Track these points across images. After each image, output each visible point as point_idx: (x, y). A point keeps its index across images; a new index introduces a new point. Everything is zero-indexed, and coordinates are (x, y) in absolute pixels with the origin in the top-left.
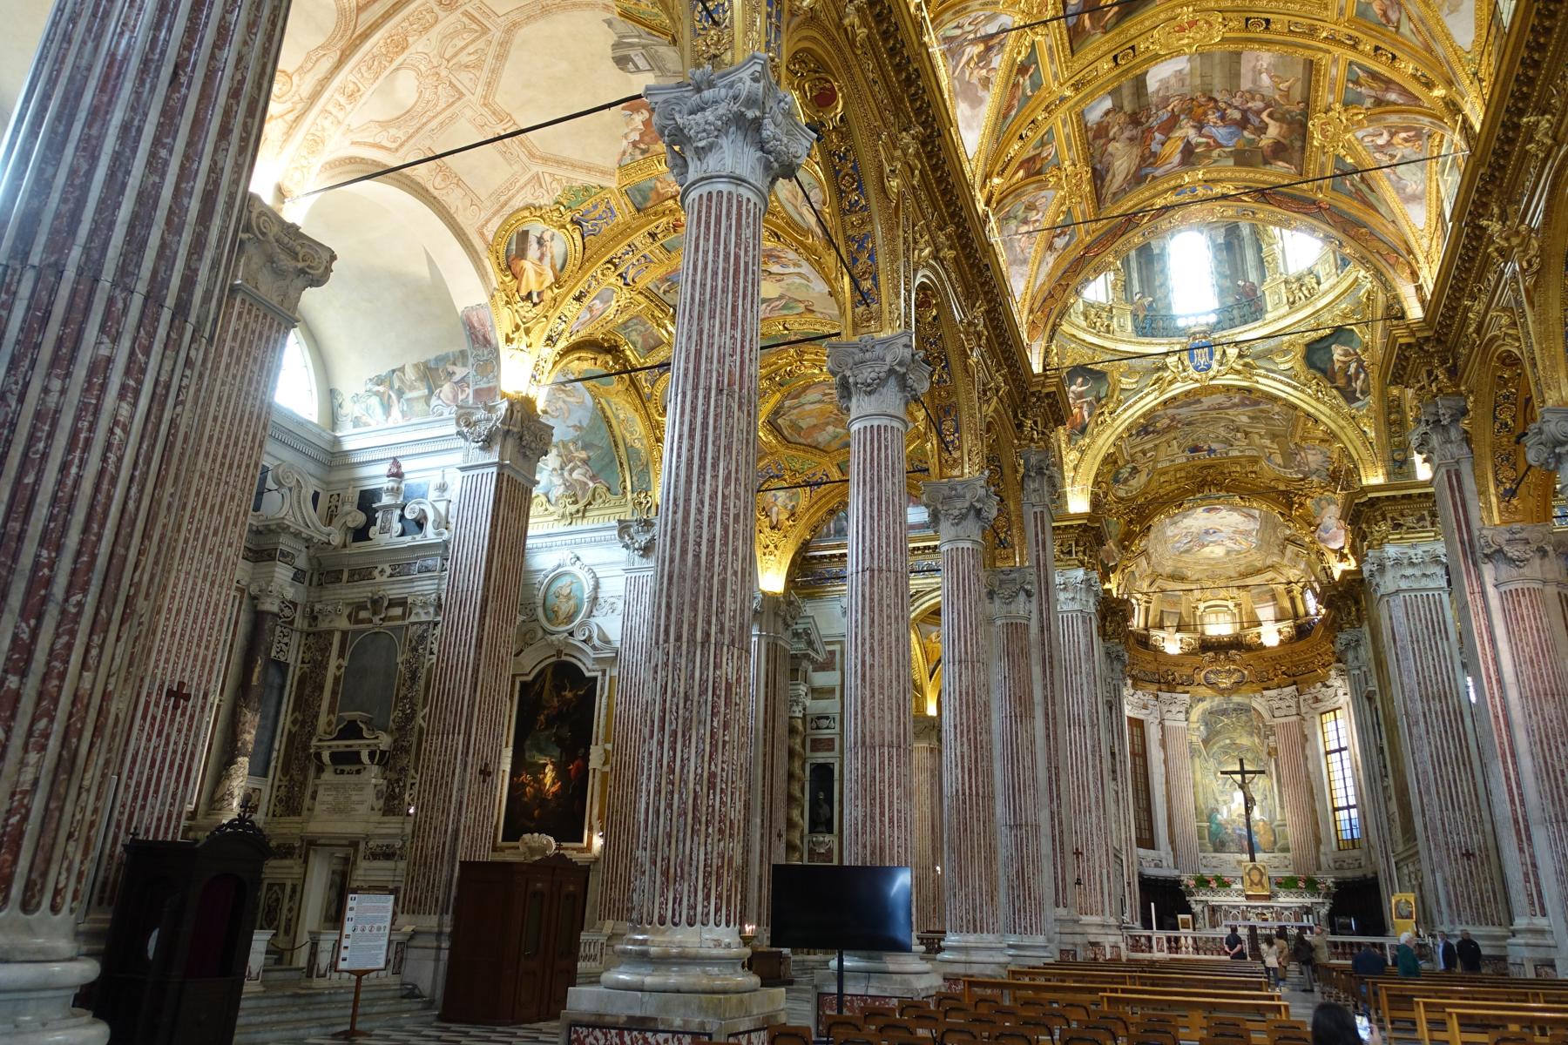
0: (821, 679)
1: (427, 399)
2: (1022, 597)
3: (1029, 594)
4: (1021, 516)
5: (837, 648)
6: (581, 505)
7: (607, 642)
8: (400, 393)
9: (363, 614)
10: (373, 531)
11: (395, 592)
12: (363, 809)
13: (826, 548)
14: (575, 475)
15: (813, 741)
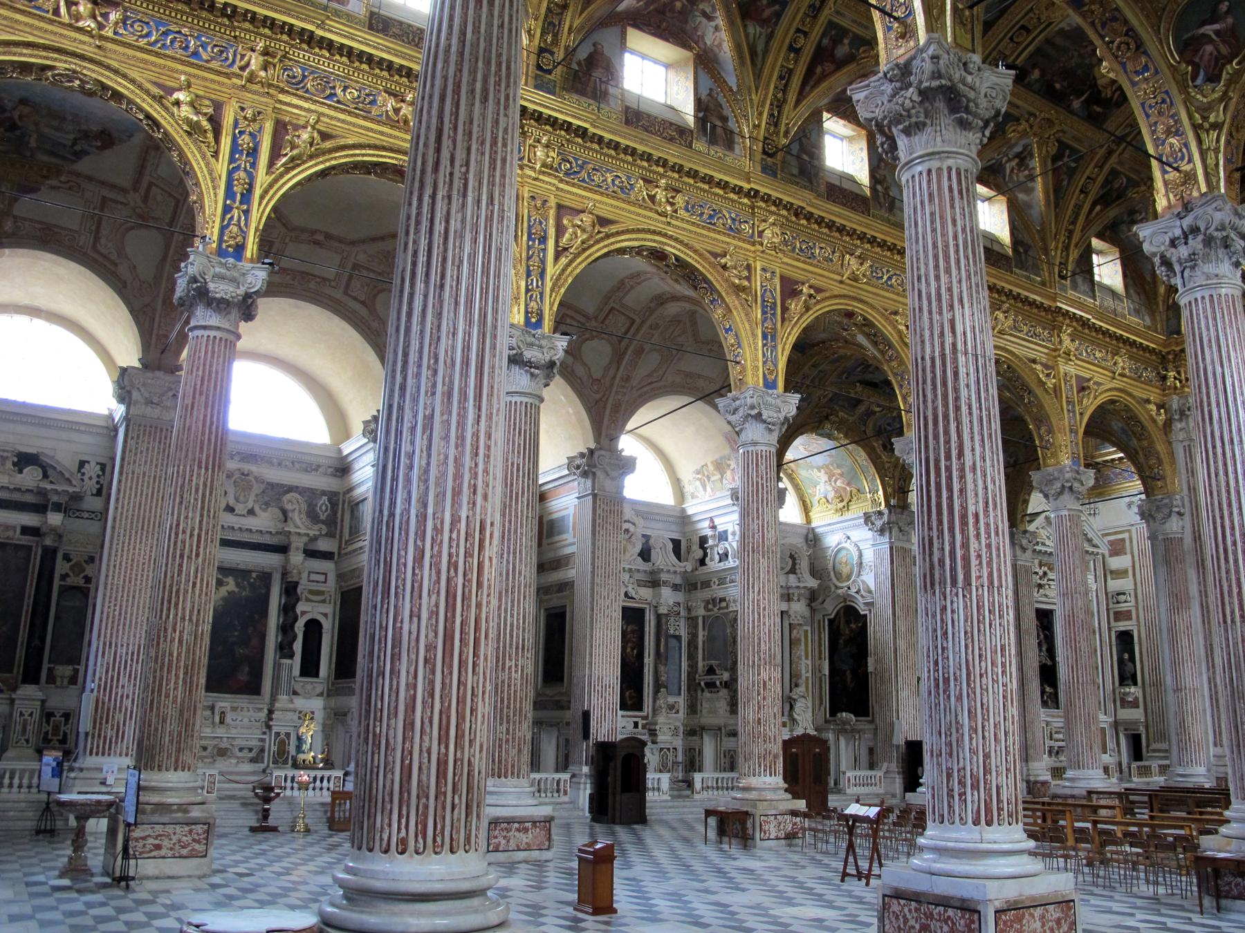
0: (1116, 563)
1: (721, 480)
2: (1174, 518)
3: (1180, 514)
4: (1172, 454)
5: (1126, 535)
6: (844, 503)
7: (870, 592)
8: (708, 478)
9: (710, 606)
10: (707, 560)
11: (721, 594)
12: (721, 711)
13: (1107, 454)
14: (839, 483)
15: (1116, 613)
